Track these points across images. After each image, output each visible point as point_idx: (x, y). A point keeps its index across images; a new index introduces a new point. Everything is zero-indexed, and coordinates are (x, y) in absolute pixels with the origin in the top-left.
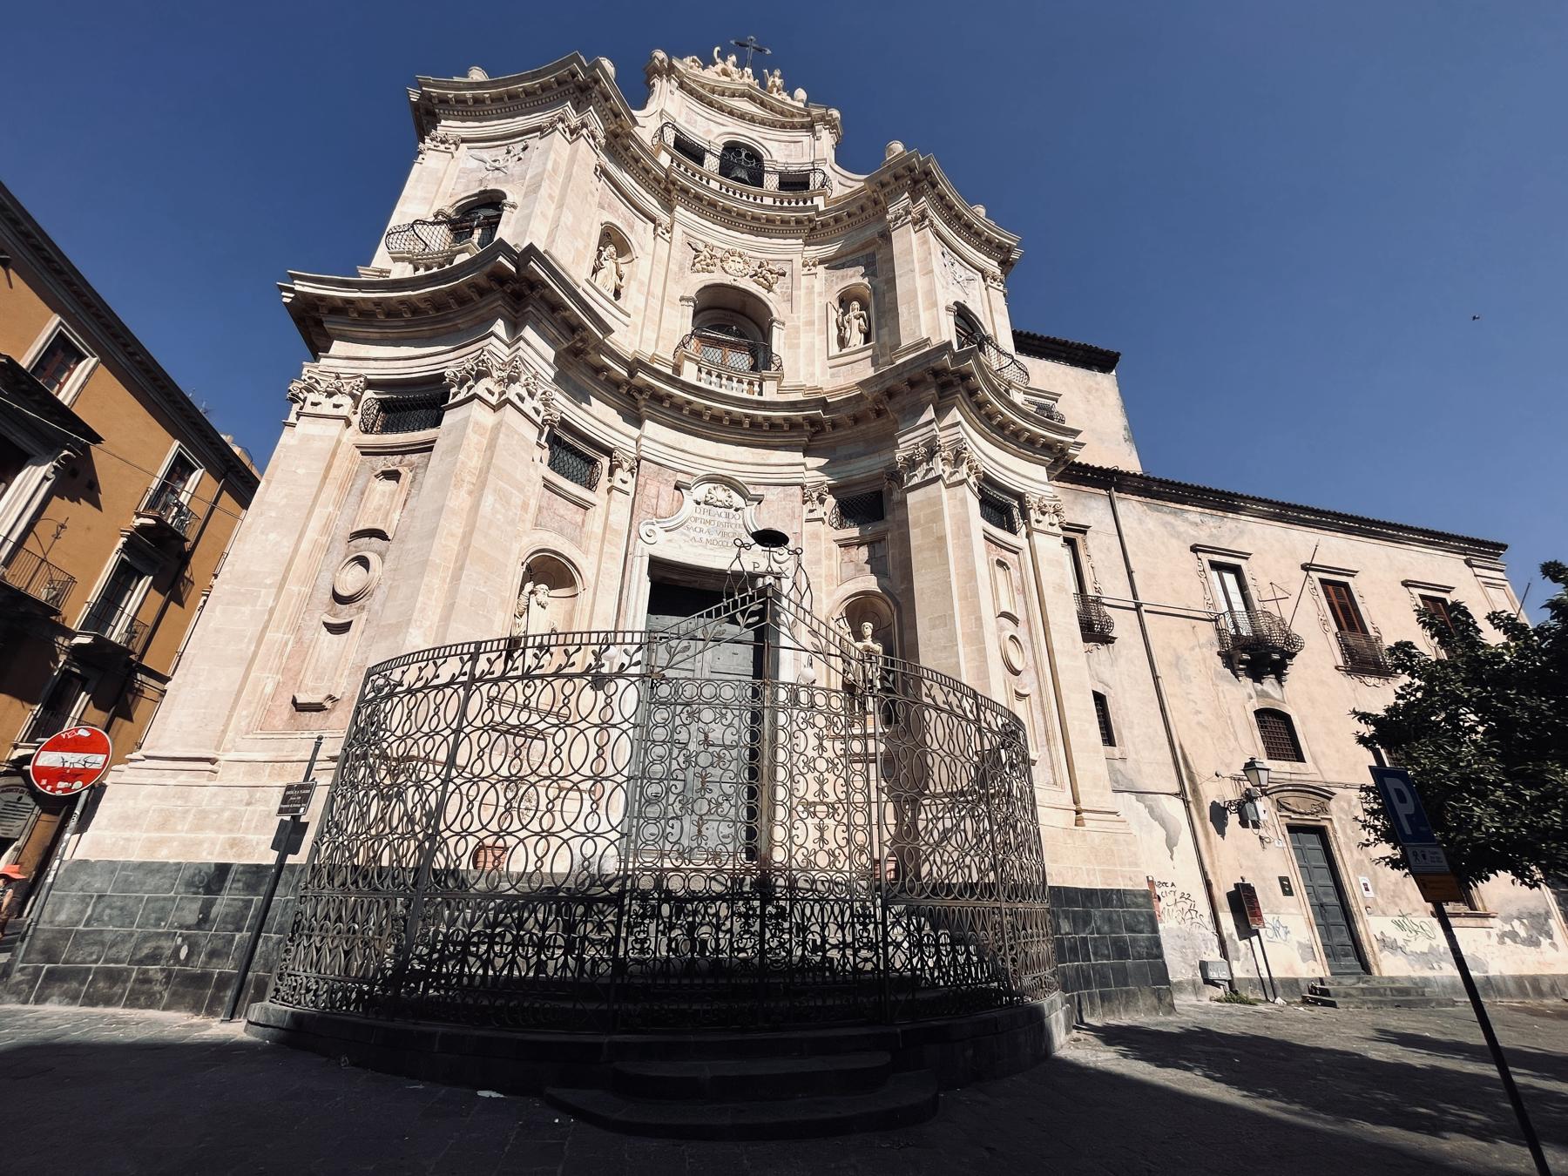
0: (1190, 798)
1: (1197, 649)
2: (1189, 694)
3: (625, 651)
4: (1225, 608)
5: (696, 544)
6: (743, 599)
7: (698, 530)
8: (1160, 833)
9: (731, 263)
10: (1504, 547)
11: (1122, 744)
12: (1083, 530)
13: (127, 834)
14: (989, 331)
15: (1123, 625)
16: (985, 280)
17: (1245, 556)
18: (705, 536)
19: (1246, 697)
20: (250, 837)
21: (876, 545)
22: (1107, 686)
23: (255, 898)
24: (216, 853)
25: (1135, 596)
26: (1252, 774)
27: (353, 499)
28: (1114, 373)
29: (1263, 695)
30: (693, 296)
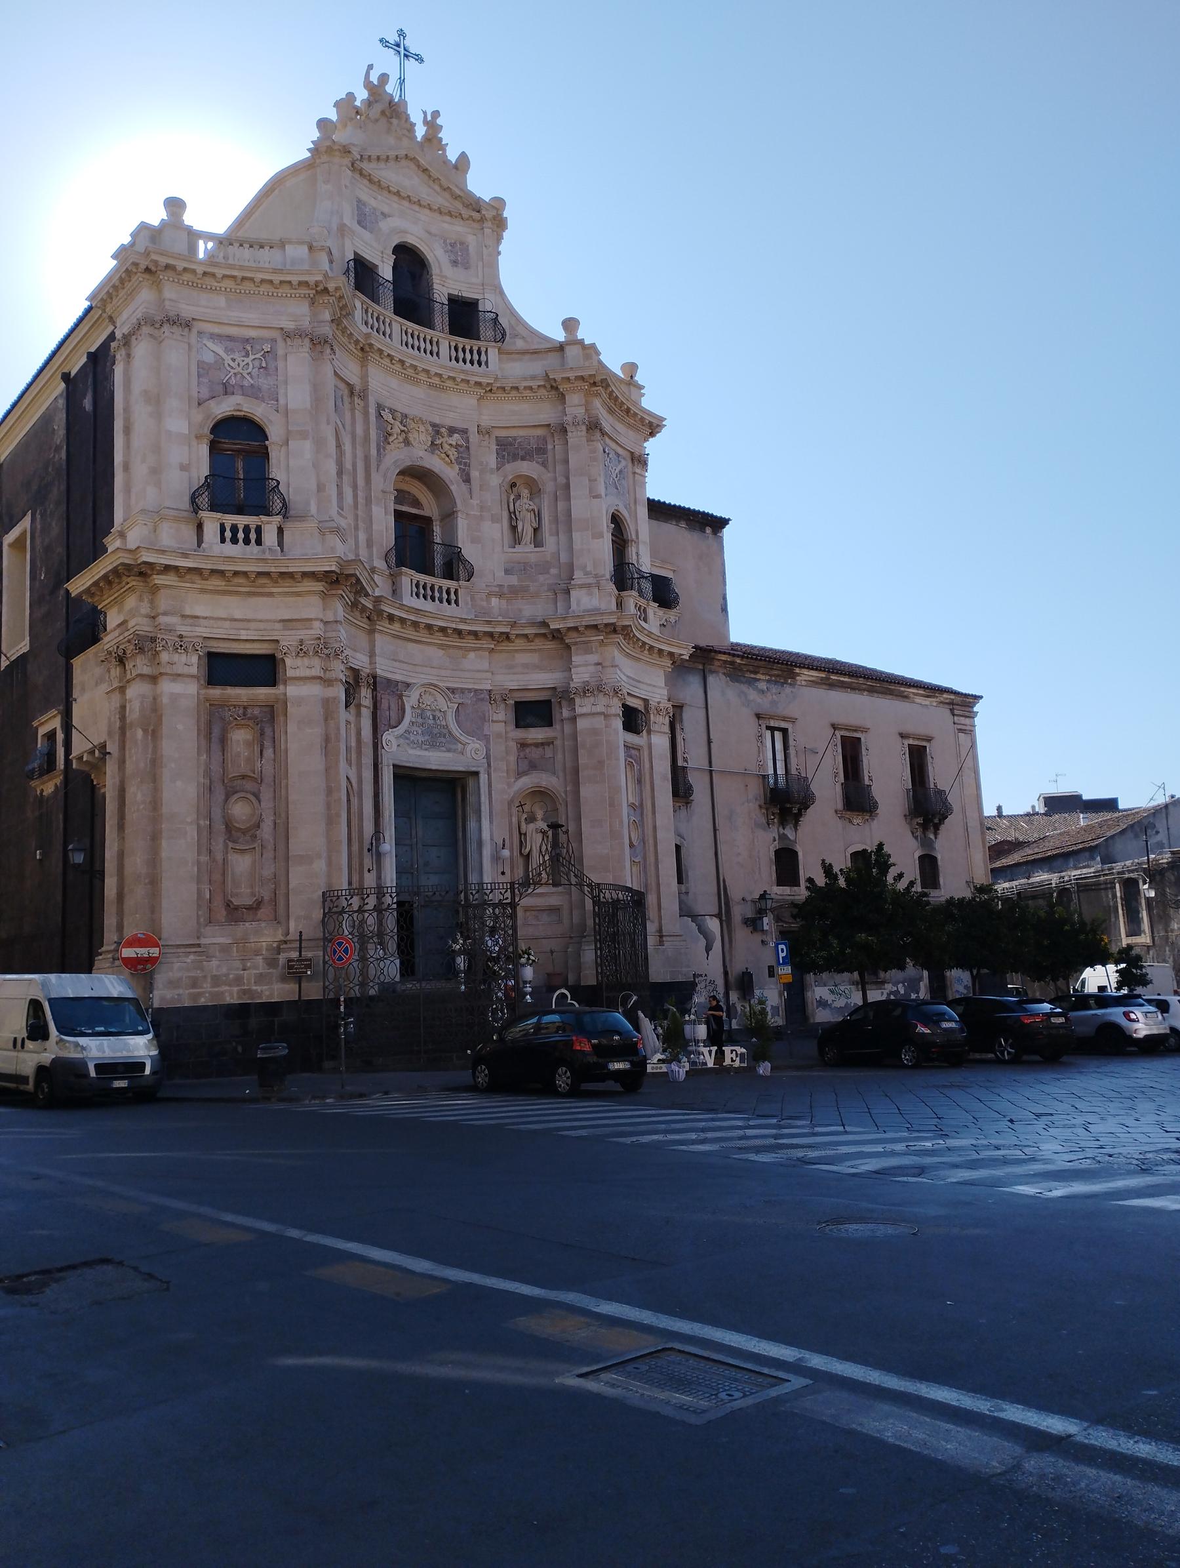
0: (724, 918)
1: (746, 804)
3: (501, 893)
4: (771, 771)
5: (415, 746)
7: (415, 733)
8: (703, 942)
9: (416, 435)
10: (981, 697)
11: (687, 883)
13: (177, 992)
14: (634, 537)
17: (793, 721)
18: (421, 738)
19: (772, 838)
20: (254, 988)
21: (546, 747)
22: (683, 838)
23: (276, 1019)
24: (235, 998)
25: (710, 762)
26: (763, 902)
27: (216, 747)
29: (783, 837)
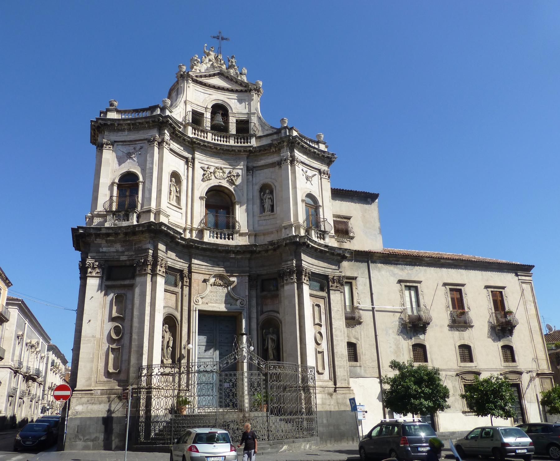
2: (388, 340)
6: (237, 352)
9: (218, 173)
10: (534, 266)
12: (355, 278)
14: (321, 204)
15: (366, 317)
16: (321, 175)
17: (420, 282)
28: (377, 201)
30: (204, 196)
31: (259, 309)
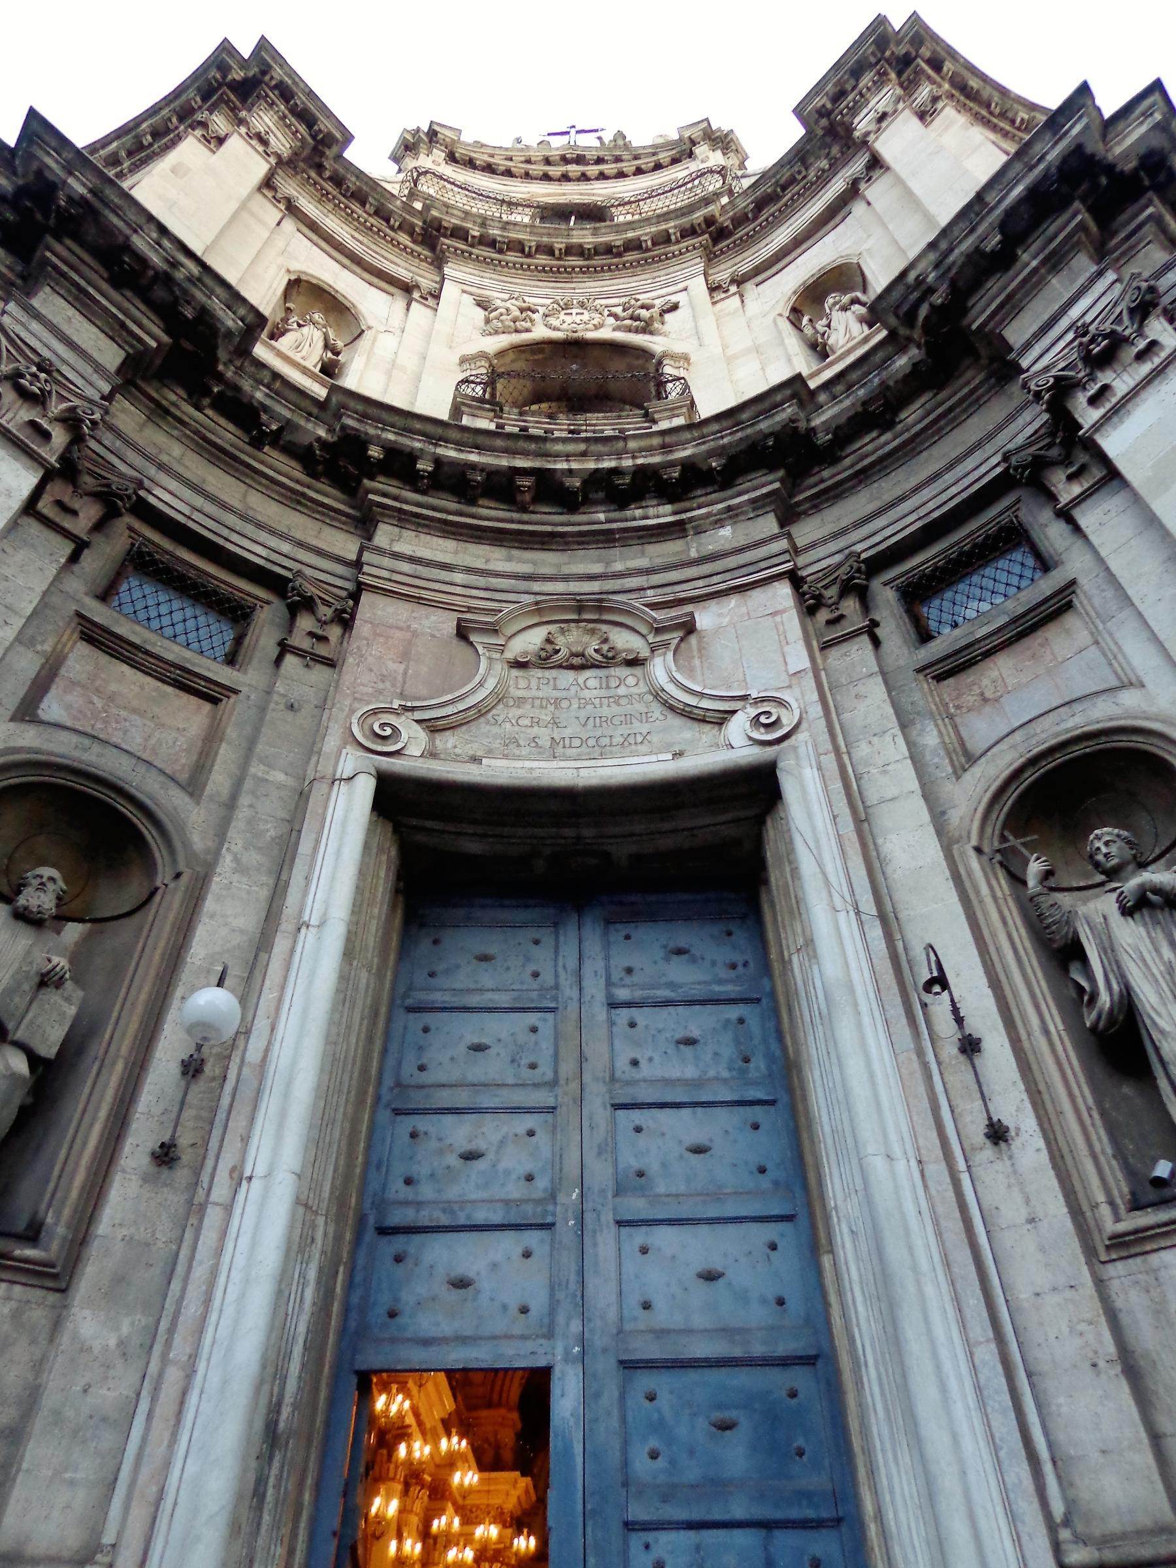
31: (930, 738)
